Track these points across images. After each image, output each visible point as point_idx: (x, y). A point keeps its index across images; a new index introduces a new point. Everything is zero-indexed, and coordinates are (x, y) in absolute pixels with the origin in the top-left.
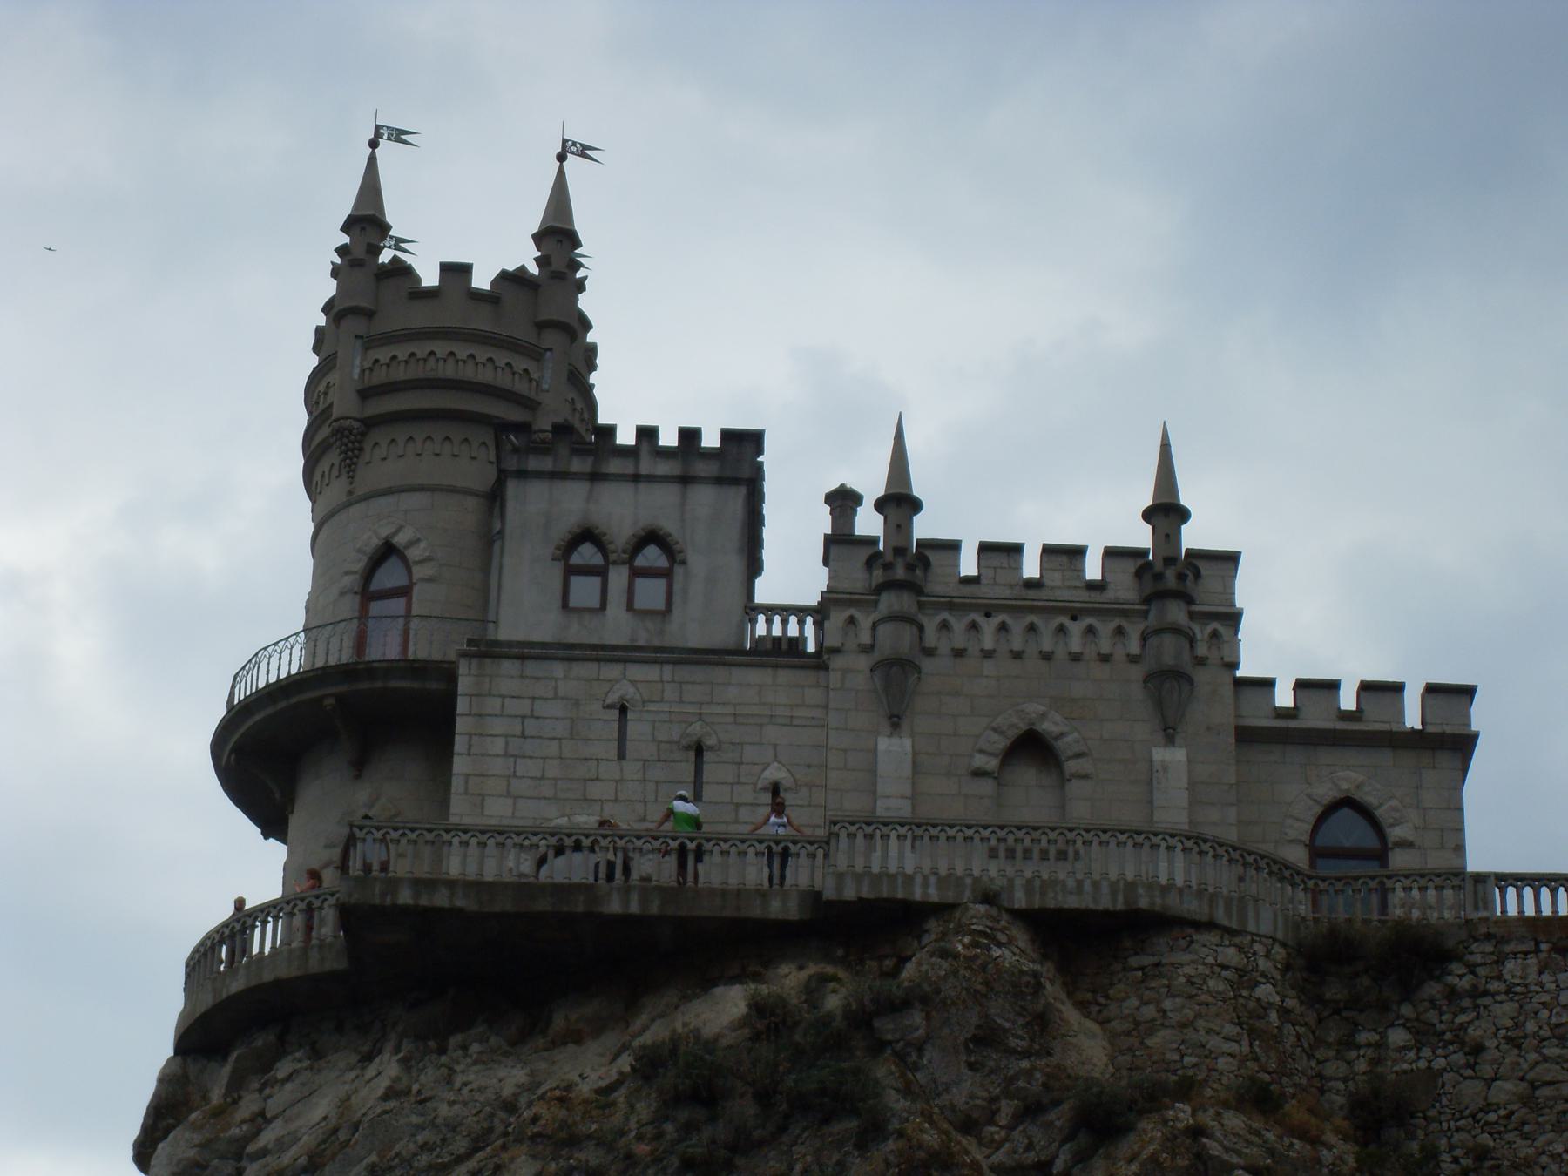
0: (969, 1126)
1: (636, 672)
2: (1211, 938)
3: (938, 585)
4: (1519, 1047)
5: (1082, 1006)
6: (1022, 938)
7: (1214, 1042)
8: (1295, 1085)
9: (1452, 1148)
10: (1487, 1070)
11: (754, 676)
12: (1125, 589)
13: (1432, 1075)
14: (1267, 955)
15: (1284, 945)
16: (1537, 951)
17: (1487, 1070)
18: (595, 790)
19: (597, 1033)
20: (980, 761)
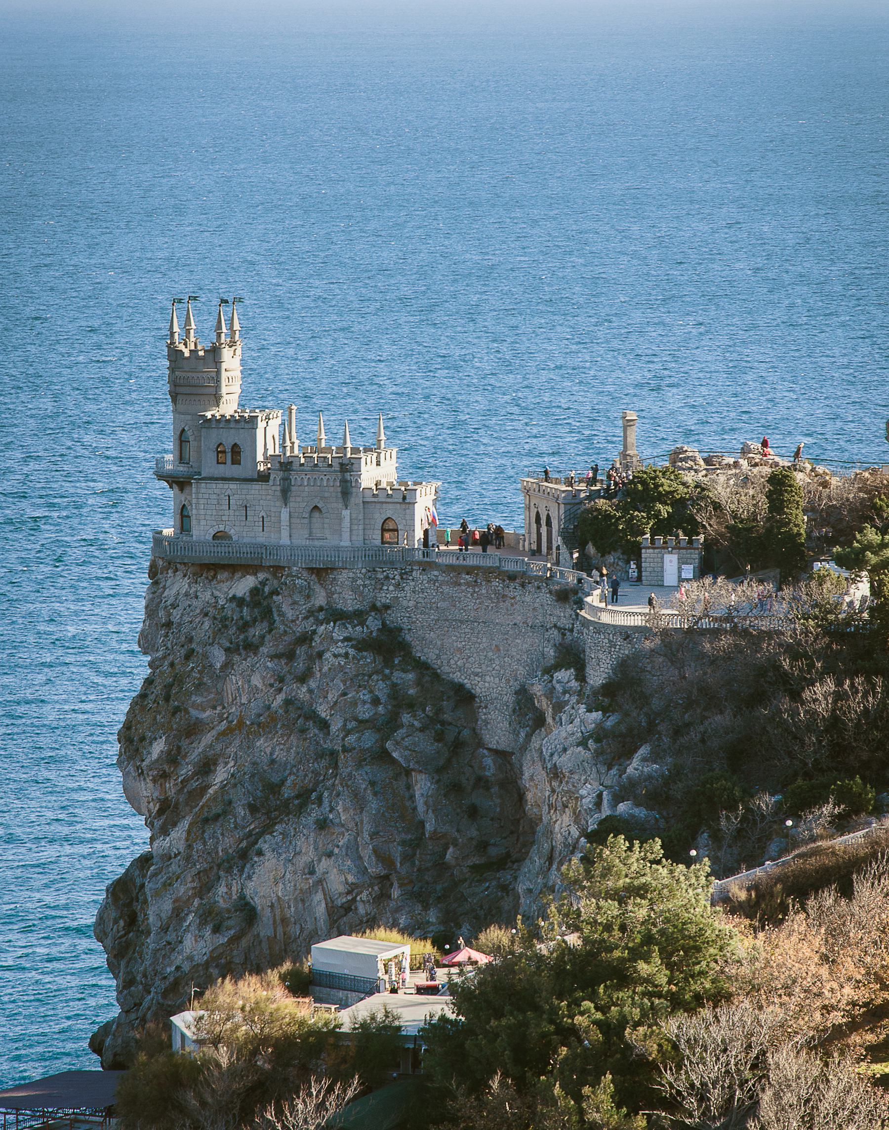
0: (293, 621)
1: (232, 486)
2: (346, 571)
3: (295, 466)
5: (321, 584)
6: (305, 574)
7: (346, 596)
11: (257, 487)
12: (336, 467)
18: (224, 518)
19: (227, 580)
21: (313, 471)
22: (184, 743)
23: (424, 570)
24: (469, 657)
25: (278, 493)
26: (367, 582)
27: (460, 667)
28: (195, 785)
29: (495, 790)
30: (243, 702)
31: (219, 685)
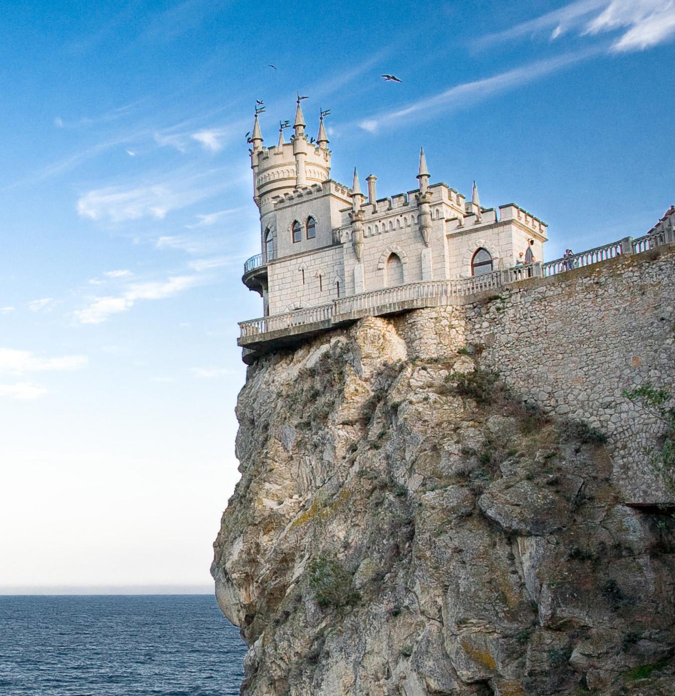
1: (308, 258)
4: (515, 323)
5: (400, 335)
8: (455, 346)
9: (499, 356)
10: (507, 331)
13: (493, 334)
14: (445, 311)
15: (451, 305)
16: (520, 291)
17: (507, 331)
20: (380, 266)
21: (387, 214)
22: (264, 540)
23: (526, 291)
24: (595, 385)
25: (351, 250)
26: (455, 322)
27: (583, 402)
28: (273, 584)
29: (644, 560)
30: (317, 485)
31: (294, 470)
